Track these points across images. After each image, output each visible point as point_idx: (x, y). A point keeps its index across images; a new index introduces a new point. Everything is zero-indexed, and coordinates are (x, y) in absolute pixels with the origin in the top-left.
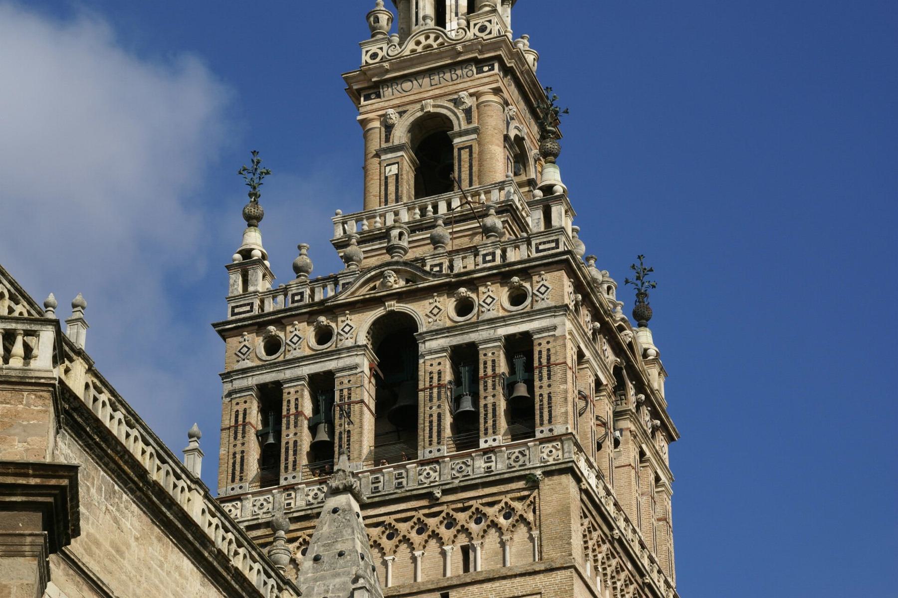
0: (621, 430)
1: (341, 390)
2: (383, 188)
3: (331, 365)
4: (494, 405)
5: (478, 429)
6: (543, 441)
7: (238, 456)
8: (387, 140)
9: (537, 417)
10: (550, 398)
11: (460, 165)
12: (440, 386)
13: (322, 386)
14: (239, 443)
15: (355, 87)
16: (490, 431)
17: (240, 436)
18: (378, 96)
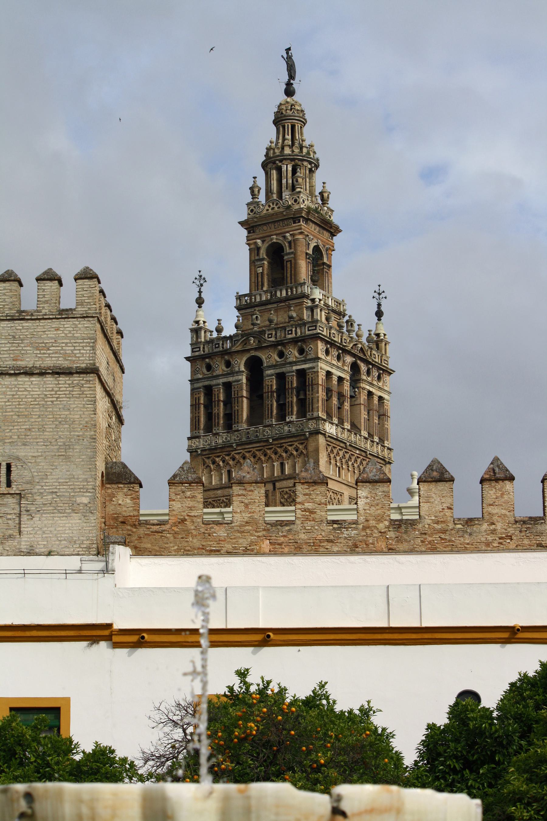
0: (358, 388)
1: (234, 391)
3: (231, 379)
4: (292, 402)
6: (309, 419)
7: (197, 418)
8: (258, 254)
9: (308, 408)
10: (312, 400)
12: (272, 392)
13: (228, 386)
16: (290, 413)
17: (197, 409)
18: (254, 232)
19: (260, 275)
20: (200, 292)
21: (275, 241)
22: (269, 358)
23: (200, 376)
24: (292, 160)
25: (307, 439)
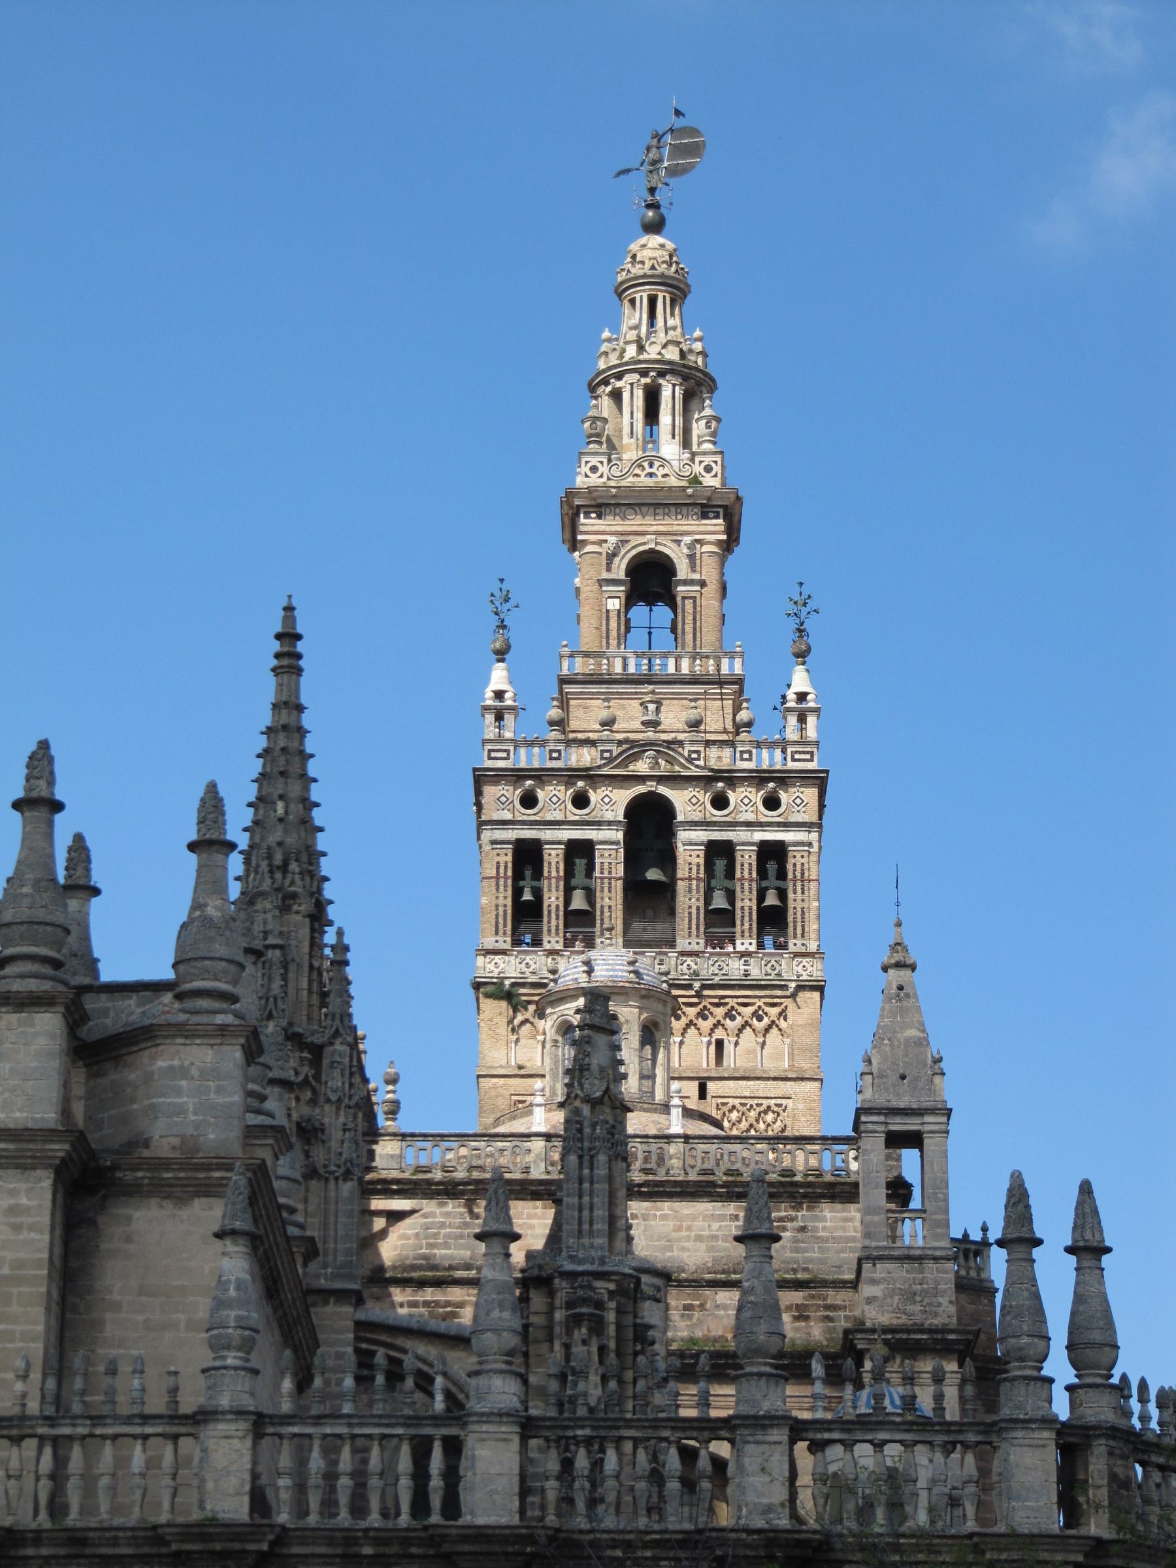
2: (604, 622)
5: (734, 926)
7: (501, 909)
8: (609, 569)
11: (684, 616)
12: (698, 879)
14: (501, 895)
15: (577, 503)
16: (747, 934)
17: (502, 888)
18: (599, 517)
19: (613, 616)
20: (503, 626)
21: (652, 546)
22: (686, 802)
23: (508, 816)
24: (685, 378)
25: (793, 996)
